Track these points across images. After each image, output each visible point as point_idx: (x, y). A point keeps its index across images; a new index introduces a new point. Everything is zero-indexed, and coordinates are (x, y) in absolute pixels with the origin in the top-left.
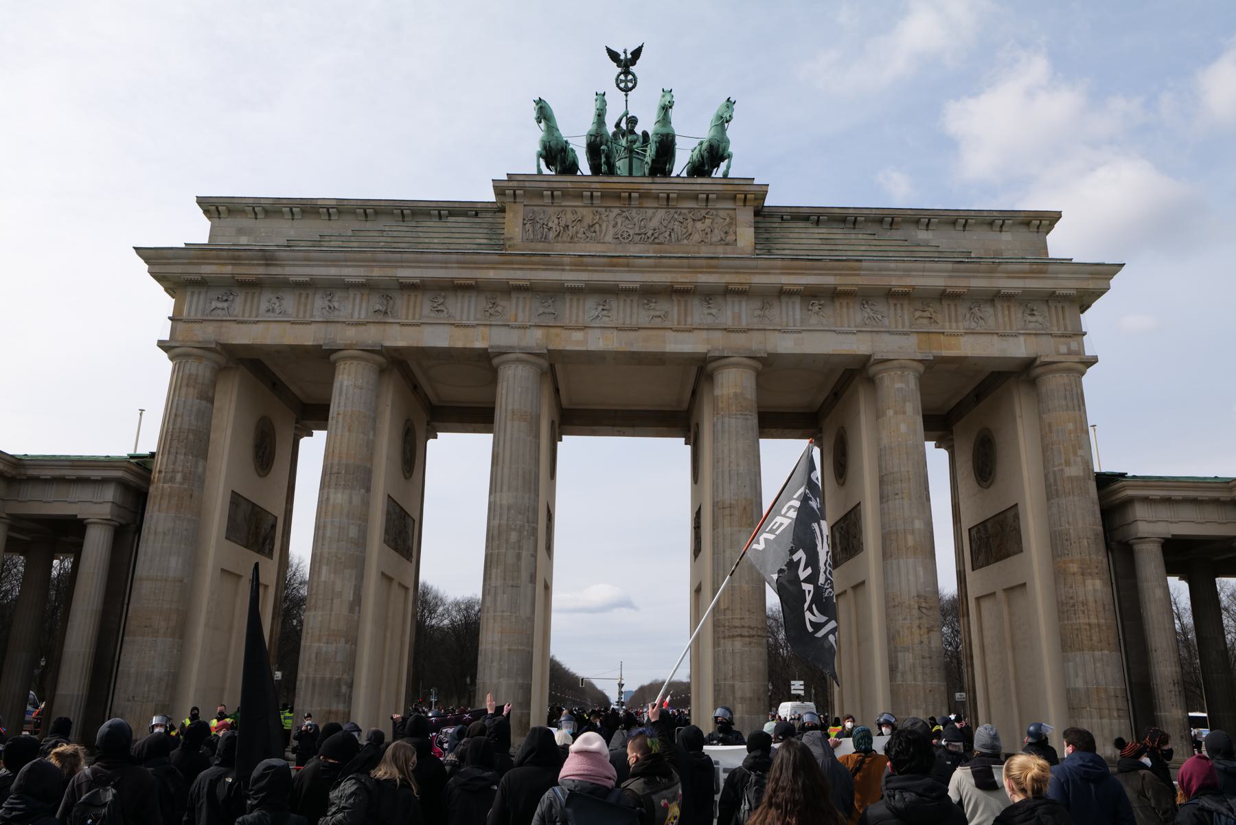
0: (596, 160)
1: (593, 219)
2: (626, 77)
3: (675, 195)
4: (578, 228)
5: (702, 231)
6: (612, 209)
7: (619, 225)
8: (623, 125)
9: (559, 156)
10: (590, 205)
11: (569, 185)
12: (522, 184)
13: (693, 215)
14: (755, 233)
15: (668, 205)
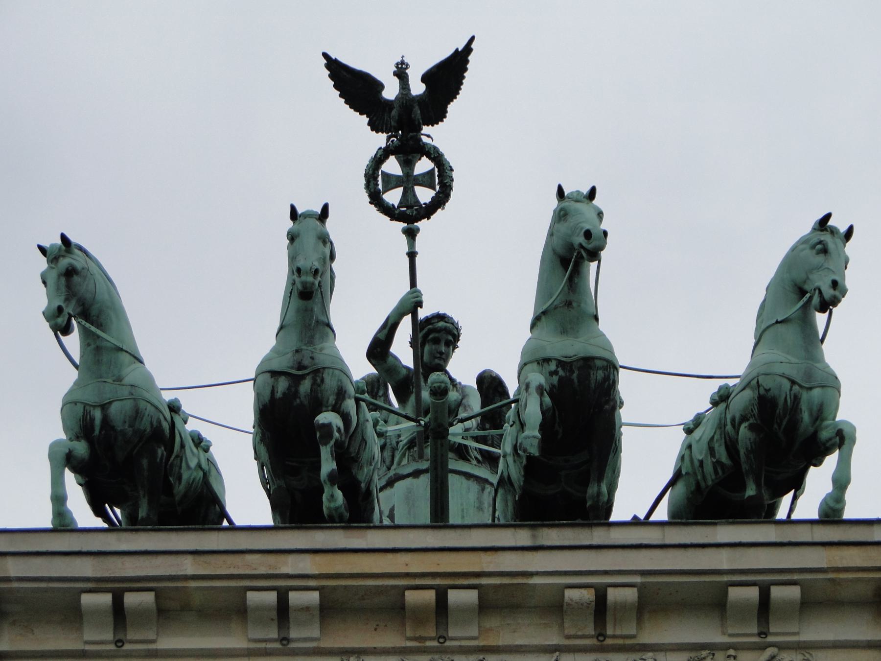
2: (407, 164)
3: (630, 595)
9: (145, 462)
10: (277, 645)
11: (188, 566)
15: (601, 635)
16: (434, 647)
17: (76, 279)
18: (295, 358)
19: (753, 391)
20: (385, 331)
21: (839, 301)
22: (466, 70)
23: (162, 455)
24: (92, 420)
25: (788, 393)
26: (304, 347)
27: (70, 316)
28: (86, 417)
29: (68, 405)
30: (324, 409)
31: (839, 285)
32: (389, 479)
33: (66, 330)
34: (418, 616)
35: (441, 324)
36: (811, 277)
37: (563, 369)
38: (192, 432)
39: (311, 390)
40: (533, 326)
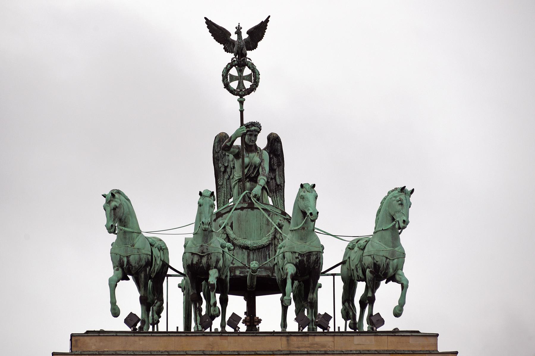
2: (240, 71)
9: (143, 275)
17: (117, 209)
20: (230, 143)
22: (266, 29)
23: (149, 269)
24: (123, 262)
25: (385, 263)
26: (204, 244)
27: (115, 227)
28: (121, 261)
30: (211, 268)
35: (253, 128)
36: (396, 214)
37: (301, 256)
39: (207, 262)
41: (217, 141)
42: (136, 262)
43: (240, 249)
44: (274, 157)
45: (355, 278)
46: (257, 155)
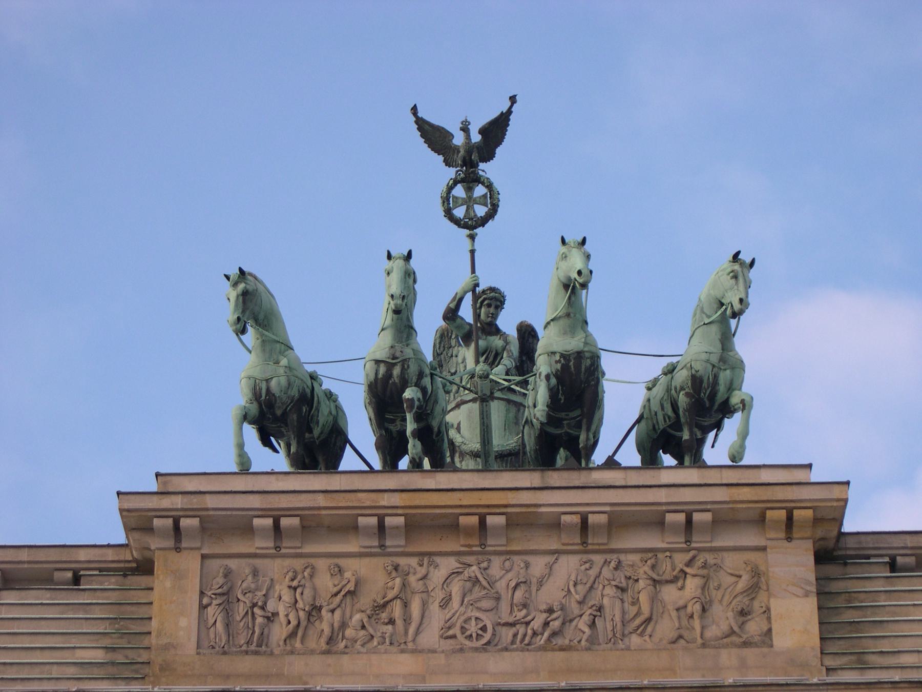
0: (393, 421)
1: (387, 588)
2: (469, 190)
3: (603, 518)
4: (348, 614)
5: (678, 610)
6: (438, 559)
7: (455, 603)
8: (466, 313)
9: (295, 417)
10: (378, 550)
11: (321, 500)
12: (195, 502)
13: (653, 567)
14: (820, 608)
15: (584, 543)
16: (478, 551)
18: (391, 352)
19: (688, 371)
21: (744, 312)
22: (508, 125)
23: (306, 408)
24: (261, 389)
25: (710, 373)
26: (396, 344)
29: (245, 379)
30: (409, 385)
31: (744, 301)
32: (457, 403)
33: (243, 331)
34: (468, 532)
35: (492, 294)
36: (726, 295)
38: (325, 389)
39: (401, 373)
40: (545, 327)
41: (438, 335)
42: (283, 389)
43: (471, 459)
44: (528, 362)
45: (660, 423)
46: (500, 339)
